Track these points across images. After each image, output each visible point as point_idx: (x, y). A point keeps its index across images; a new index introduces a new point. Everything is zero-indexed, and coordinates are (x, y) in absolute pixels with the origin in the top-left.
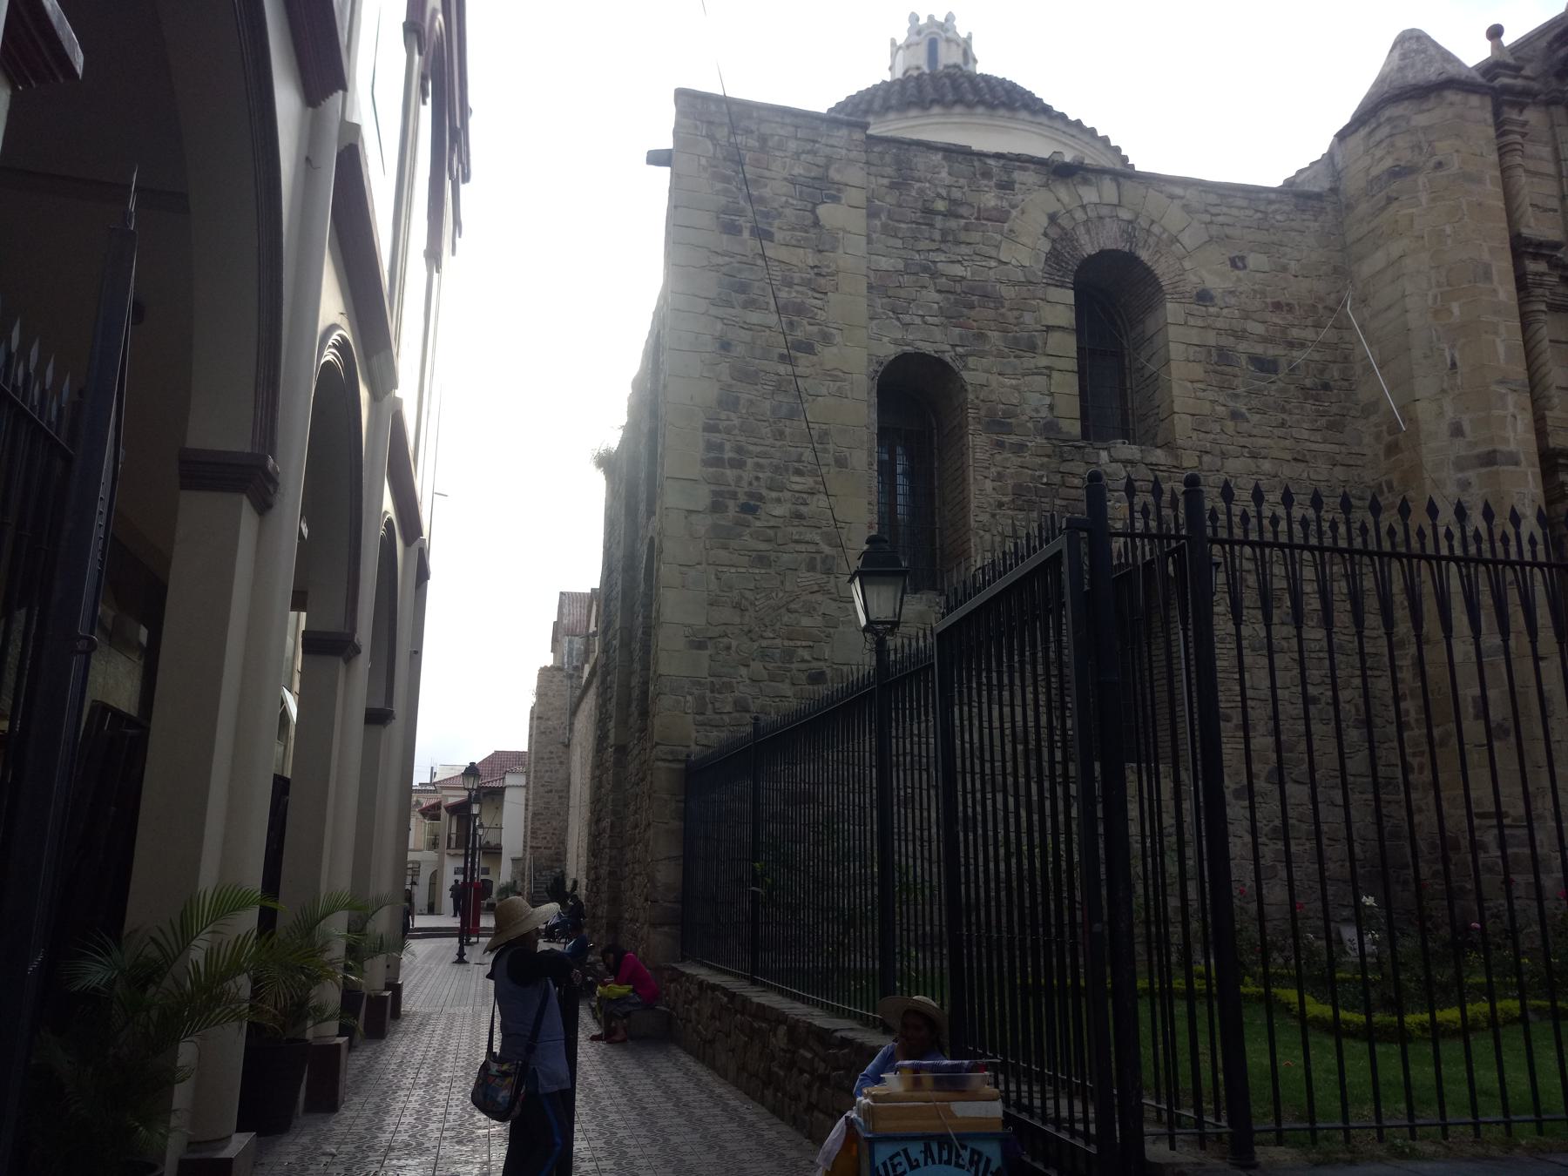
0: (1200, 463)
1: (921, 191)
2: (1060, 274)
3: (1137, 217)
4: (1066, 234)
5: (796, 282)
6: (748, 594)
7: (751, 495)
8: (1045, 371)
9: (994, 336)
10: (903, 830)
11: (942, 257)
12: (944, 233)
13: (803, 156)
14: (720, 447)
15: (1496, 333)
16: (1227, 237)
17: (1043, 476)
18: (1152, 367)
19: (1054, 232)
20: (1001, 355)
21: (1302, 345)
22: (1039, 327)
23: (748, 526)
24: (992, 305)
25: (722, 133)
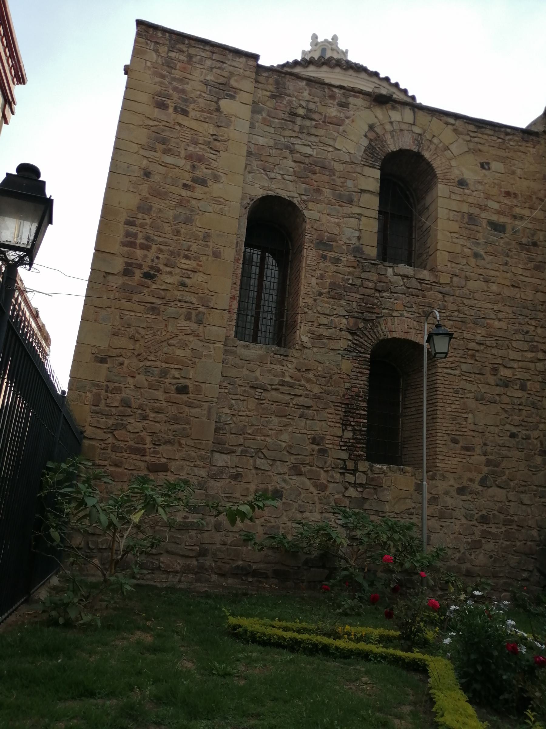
0: (451, 281)
1: (290, 102)
2: (372, 160)
3: (424, 132)
4: (379, 137)
5: (200, 142)
7: (152, 268)
8: (357, 216)
9: (327, 192)
11: (299, 141)
13: (215, 70)
16: (480, 150)
17: (348, 280)
19: (371, 135)
21: (522, 218)
22: (356, 190)
23: (147, 287)
24: (327, 173)
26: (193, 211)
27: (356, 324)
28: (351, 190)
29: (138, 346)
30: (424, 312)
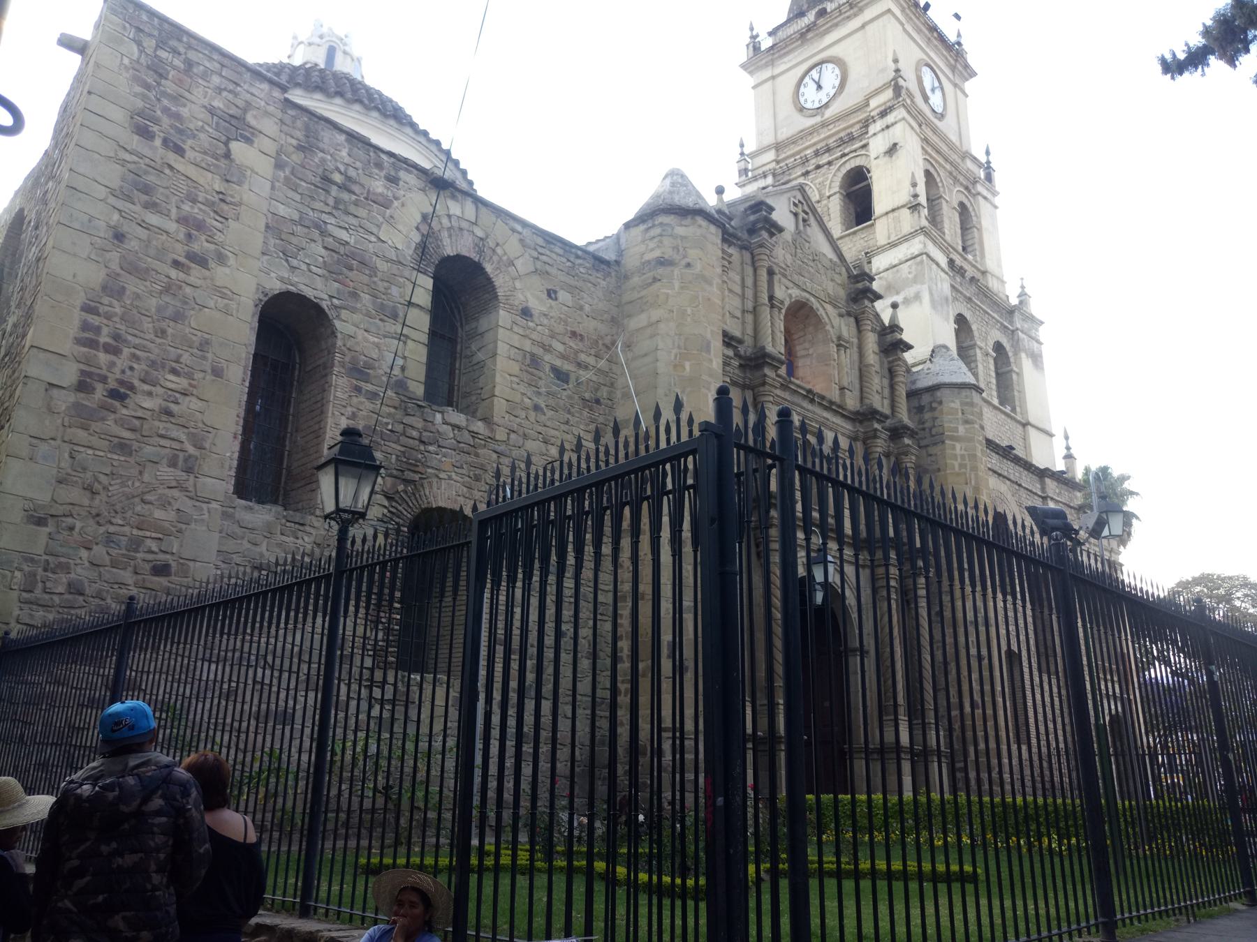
0: (508, 439)
1: (323, 161)
3: (487, 237)
4: (433, 233)
5: (200, 199)
6: (103, 478)
7: (121, 382)
9: (366, 298)
10: (220, 721)
11: (333, 221)
12: (337, 201)
13: (225, 94)
14: (98, 330)
15: (708, 389)
16: (547, 272)
17: (387, 424)
18: (480, 356)
19: (425, 229)
20: (368, 315)
23: (114, 412)
24: (367, 272)
25: (149, 44)
26: (186, 303)
27: (394, 485)
28: (396, 300)
29: (97, 502)
30: (475, 475)
